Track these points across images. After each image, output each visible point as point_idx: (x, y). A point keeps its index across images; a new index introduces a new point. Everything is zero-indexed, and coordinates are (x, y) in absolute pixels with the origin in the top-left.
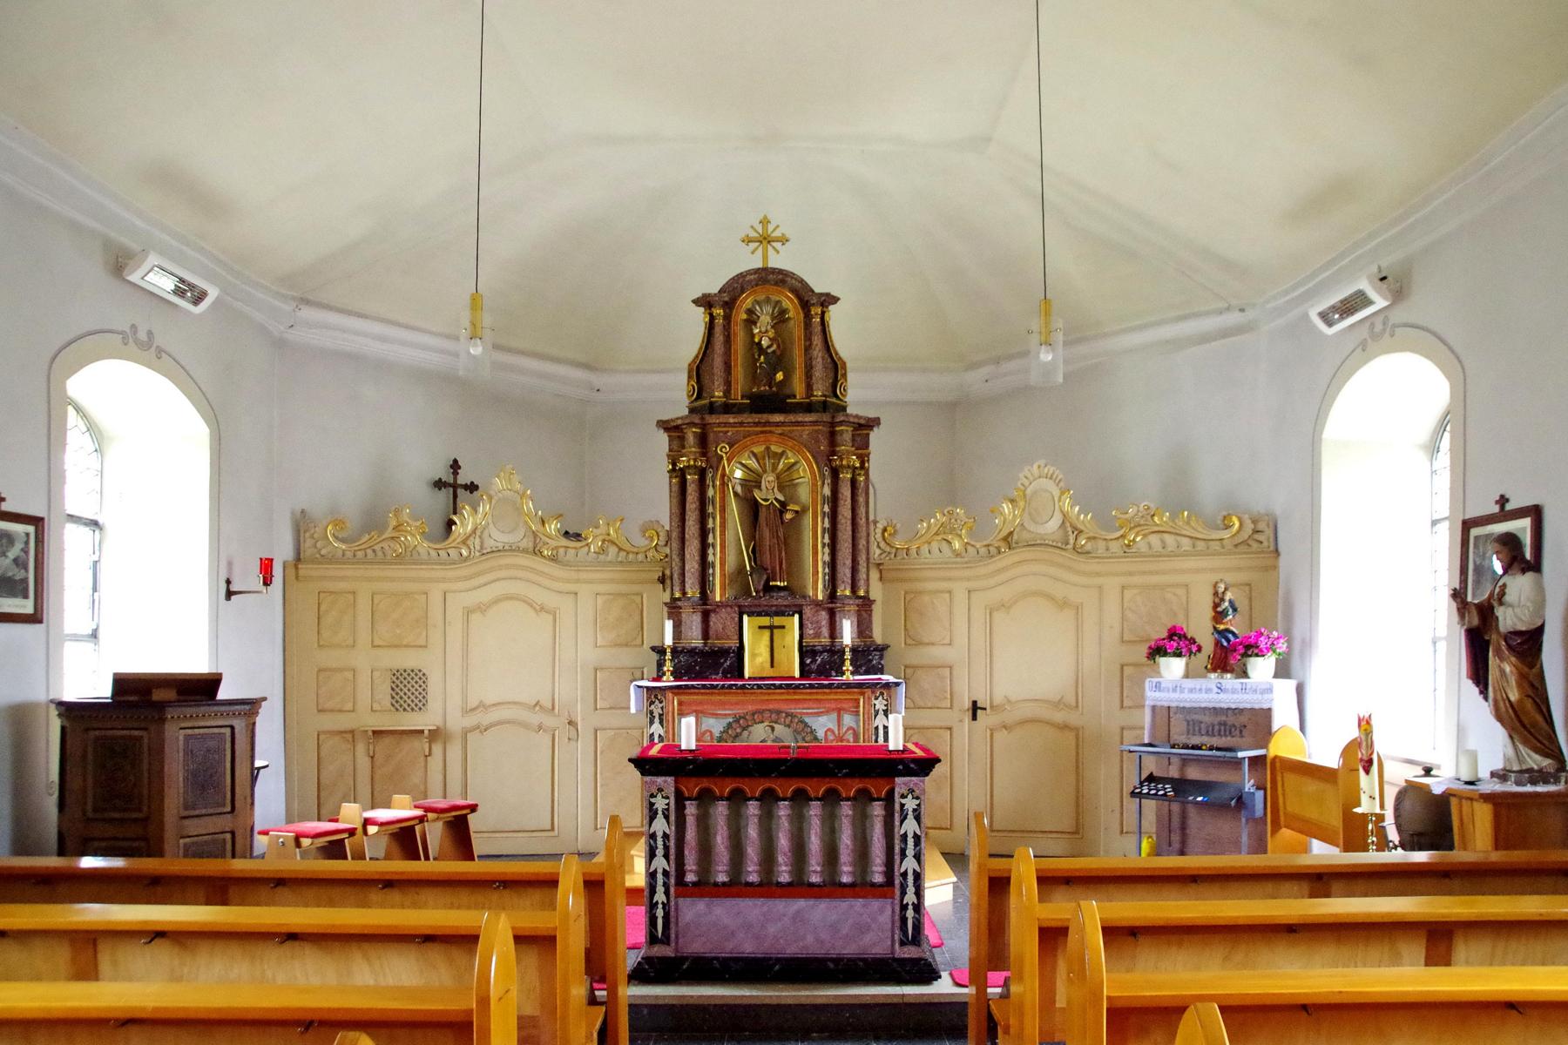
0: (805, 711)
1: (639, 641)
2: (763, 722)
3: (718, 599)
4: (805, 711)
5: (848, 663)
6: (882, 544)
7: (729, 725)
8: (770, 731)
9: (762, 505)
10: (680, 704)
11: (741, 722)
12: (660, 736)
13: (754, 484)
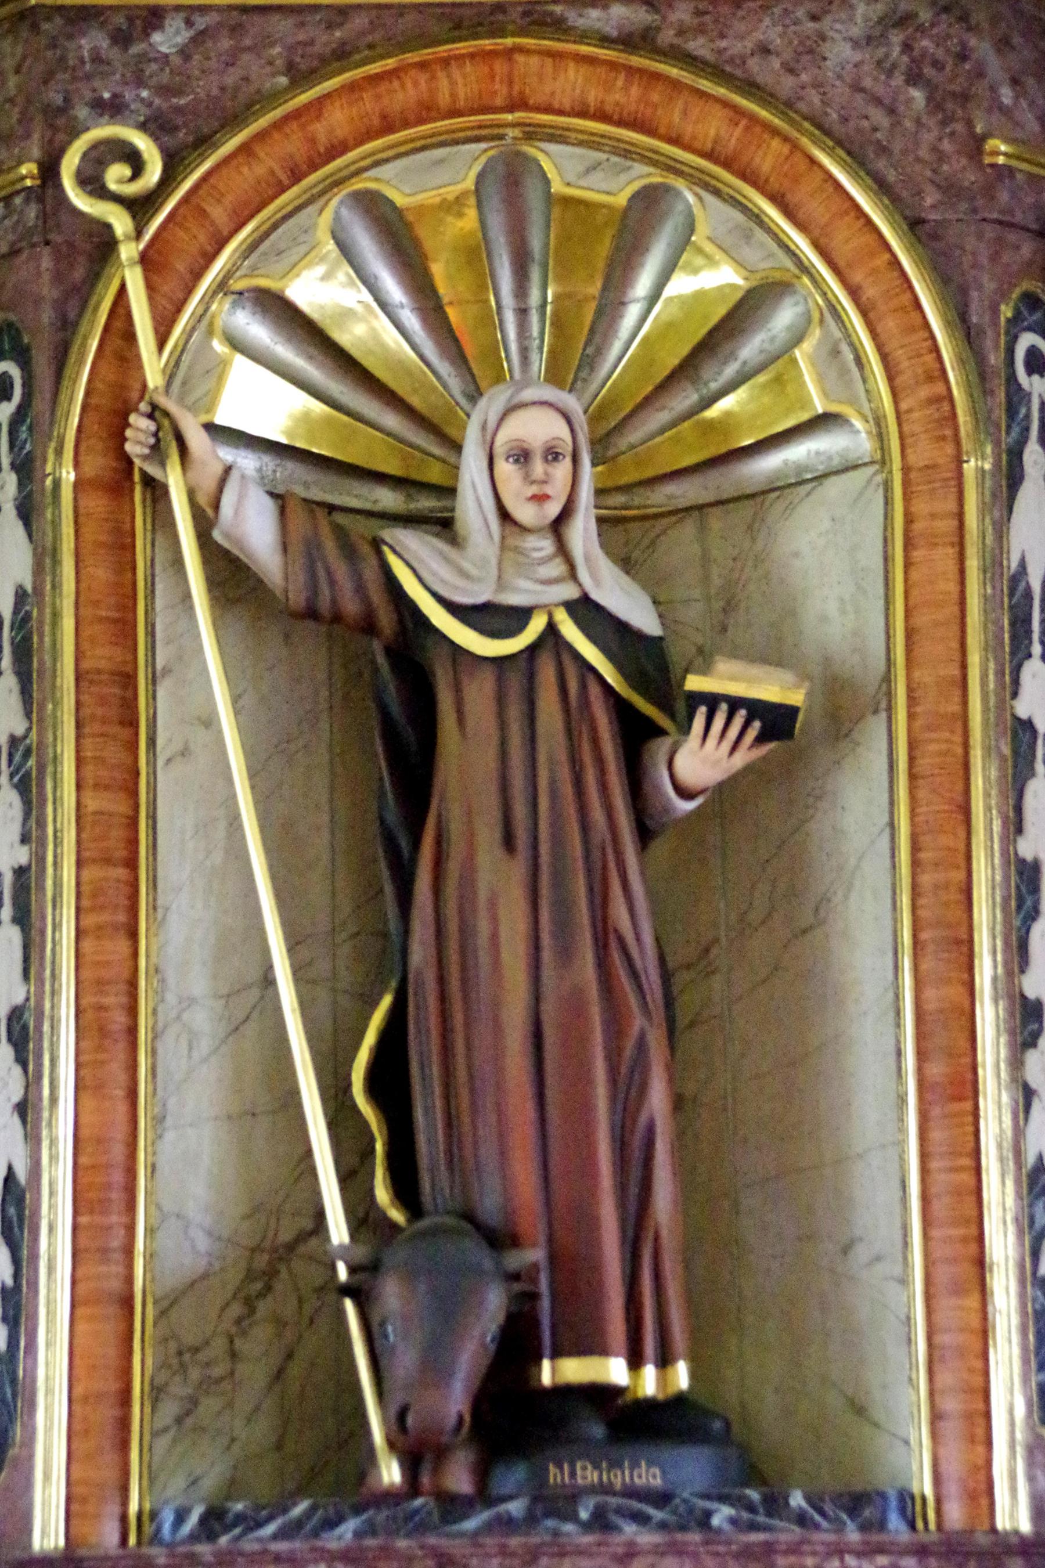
9: (457, 651)
13: (387, 499)
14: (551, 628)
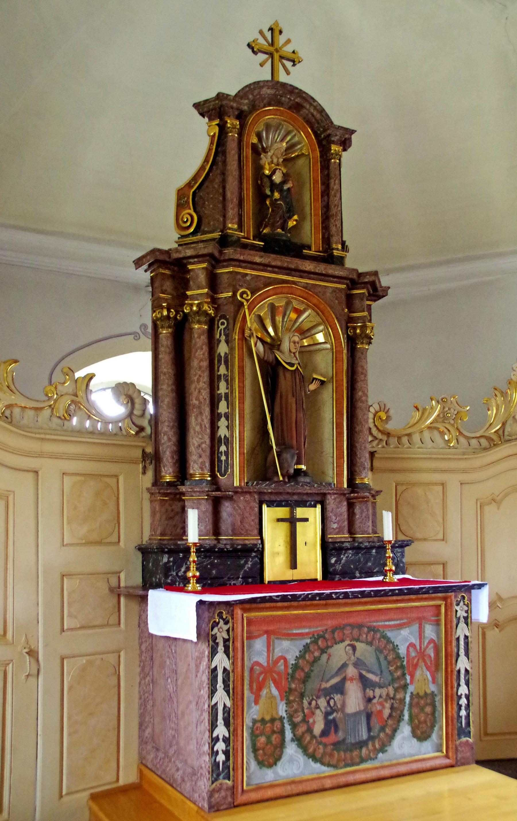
0: (387, 623)
1: (114, 539)
2: (342, 641)
3: (236, 483)
4: (387, 623)
5: (389, 562)
6: (374, 431)
7: (307, 648)
8: (351, 652)
10: (250, 622)
11: (320, 643)
12: (225, 670)
14: (297, 367)
